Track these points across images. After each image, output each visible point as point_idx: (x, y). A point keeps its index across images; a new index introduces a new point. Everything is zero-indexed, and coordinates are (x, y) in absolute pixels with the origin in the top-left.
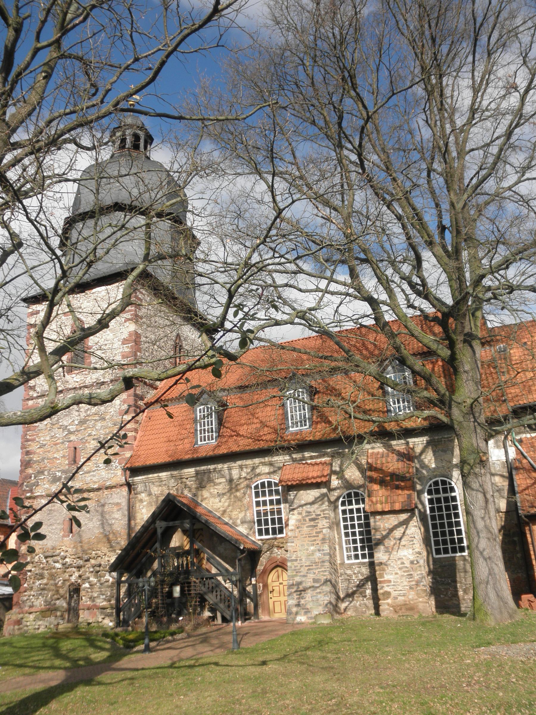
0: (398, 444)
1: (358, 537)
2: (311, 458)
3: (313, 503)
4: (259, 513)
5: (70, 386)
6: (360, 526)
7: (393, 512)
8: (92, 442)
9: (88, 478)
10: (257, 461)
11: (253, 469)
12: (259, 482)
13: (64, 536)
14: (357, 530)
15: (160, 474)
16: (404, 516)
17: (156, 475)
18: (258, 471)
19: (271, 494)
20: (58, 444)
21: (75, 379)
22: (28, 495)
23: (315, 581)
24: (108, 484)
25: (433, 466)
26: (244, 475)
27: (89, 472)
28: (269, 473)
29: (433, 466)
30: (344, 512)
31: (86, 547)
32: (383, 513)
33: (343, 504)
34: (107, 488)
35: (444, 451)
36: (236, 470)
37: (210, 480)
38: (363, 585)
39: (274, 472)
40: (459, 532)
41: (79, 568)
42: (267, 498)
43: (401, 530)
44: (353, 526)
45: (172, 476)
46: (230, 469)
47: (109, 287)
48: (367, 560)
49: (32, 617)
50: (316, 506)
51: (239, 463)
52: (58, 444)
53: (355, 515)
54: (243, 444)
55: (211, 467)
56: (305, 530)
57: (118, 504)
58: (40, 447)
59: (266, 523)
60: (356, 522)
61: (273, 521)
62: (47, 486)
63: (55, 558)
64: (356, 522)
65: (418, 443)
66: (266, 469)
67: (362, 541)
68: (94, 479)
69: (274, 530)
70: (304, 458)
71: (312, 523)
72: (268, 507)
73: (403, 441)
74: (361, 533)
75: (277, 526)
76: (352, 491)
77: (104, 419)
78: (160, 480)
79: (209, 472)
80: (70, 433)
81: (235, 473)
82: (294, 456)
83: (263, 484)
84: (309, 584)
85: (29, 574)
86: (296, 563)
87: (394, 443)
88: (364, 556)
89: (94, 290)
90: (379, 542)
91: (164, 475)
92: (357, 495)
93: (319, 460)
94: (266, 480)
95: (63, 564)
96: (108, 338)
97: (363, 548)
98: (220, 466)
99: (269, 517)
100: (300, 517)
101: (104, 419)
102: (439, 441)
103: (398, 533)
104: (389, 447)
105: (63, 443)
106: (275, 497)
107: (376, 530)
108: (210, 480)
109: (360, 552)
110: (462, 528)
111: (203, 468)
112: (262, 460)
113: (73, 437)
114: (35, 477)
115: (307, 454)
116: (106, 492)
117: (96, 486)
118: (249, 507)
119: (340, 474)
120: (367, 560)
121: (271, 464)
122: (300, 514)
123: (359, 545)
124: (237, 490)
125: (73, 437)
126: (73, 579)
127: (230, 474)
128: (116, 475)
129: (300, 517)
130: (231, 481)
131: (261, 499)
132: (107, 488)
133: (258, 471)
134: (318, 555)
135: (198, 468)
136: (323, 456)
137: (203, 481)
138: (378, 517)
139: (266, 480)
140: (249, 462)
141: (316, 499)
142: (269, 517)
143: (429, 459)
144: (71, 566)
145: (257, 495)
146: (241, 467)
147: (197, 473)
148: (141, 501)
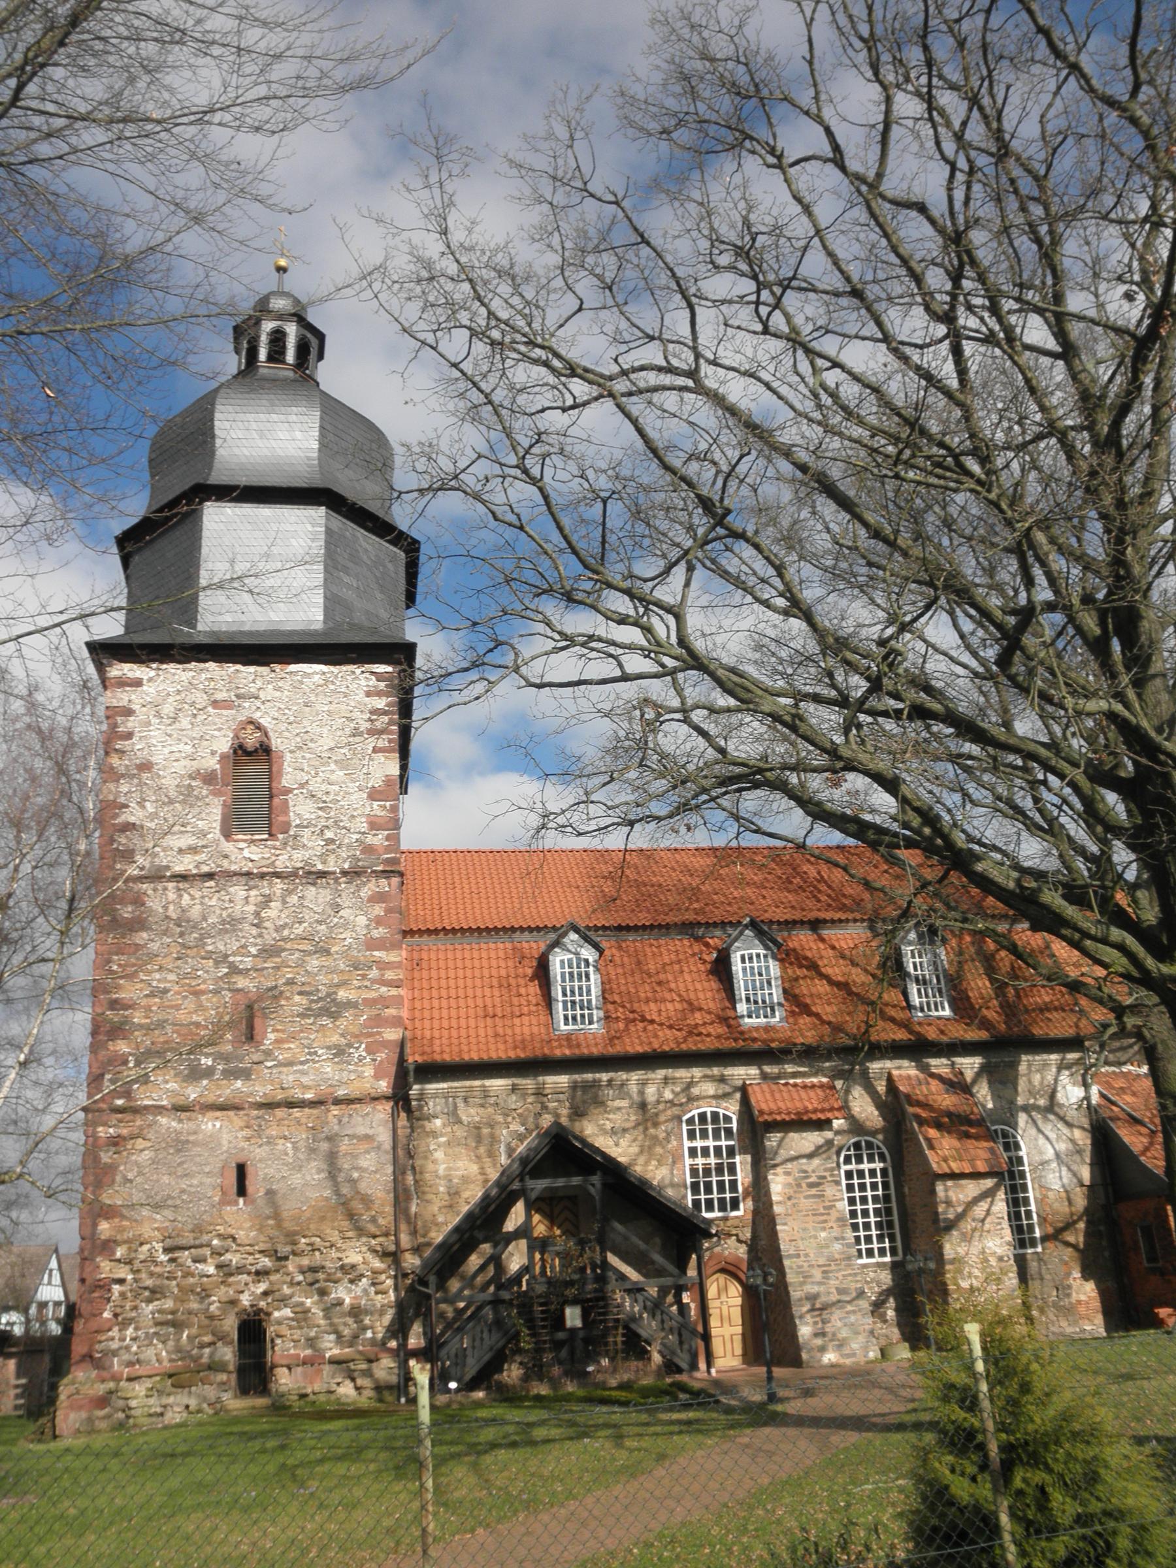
0: (939, 1065)
1: (872, 1219)
2: (795, 1075)
3: (810, 1156)
4: (694, 1171)
5: (233, 868)
6: (875, 1199)
7: (976, 1176)
8: (297, 998)
9: (288, 1077)
10: (697, 1072)
11: (690, 1085)
12: (695, 1112)
13: (223, 1202)
14: (871, 1206)
15: (488, 1082)
16: (989, 1183)
17: (477, 1083)
18: (695, 1091)
19: (717, 1137)
20: (203, 992)
21: (246, 853)
22: (120, 1102)
23: (840, 1291)
24: (341, 1092)
25: (990, 1105)
26: (668, 1095)
27: (290, 1064)
28: (715, 1097)
29: (990, 1105)
30: (849, 1175)
31: (289, 1225)
32: (953, 1176)
33: (848, 1160)
34: (337, 1102)
35: (1003, 1083)
36: (653, 1085)
37: (600, 1103)
38: (884, 1302)
39: (726, 1096)
40: (1029, 1214)
41: (261, 1274)
42: (710, 1143)
43: (984, 1205)
44: (864, 1200)
45: (514, 1089)
46: (643, 1083)
47: (335, 669)
48: (888, 1259)
49: (140, 1389)
50: (816, 1162)
51: (661, 1073)
52: (203, 992)
53: (868, 1180)
54: (666, 1040)
55: (604, 1077)
56: (805, 1204)
57: (368, 1138)
58: (152, 995)
59: (708, 1190)
60: (869, 1193)
61: (721, 1185)
62: (172, 1085)
63: (200, 1251)
64: (869, 1193)
65: (970, 1064)
66: (710, 1089)
67: (879, 1225)
68: (305, 1080)
69: (722, 1201)
70: (779, 1077)
71: (814, 1191)
72: (712, 1160)
73: (944, 1061)
74: (877, 1212)
75: (728, 1195)
76: (863, 1140)
77: (327, 952)
78: (485, 1093)
79: (596, 1084)
80: (235, 970)
81: (651, 1091)
82: (767, 1069)
83: (703, 1117)
84: (834, 1297)
85: (116, 1288)
86: (800, 1261)
87: (933, 1062)
88: (882, 1252)
89: (293, 667)
90: (950, 1226)
91: (497, 1084)
92: (870, 1145)
93: (808, 1081)
94: (709, 1110)
95: (219, 1267)
96: (333, 778)
97: (880, 1238)
98: (623, 1075)
99: (714, 1179)
100: (790, 1179)
101: (327, 952)
102: (997, 1066)
103: (980, 1210)
104: (925, 1069)
105: (216, 992)
106: (724, 1143)
107: (948, 1203)
108: (600, 1103)
109: (875, 1246)
110: (1033, 1207)
111: (589, 1076)
112: (708, 1071)
113: (241, 982)
114: (138, 1063)
115: (790, 1068)
116: (335, 1111)
117: (309, 1096)
118: (677, 1159)
119: (845, 1108)
120: (888, 1259)
121: (722, 1080)
122: (787, 1174)
123: (874, 1232)
124: (656, 1125)
125: (241, 982)
126: (245, 1300)
127: (641, 1093)
128: (360, 1077)
129: (790, 1179)
130: (643, 1106)
131: (699, 1143)
132: (337, 1102)
133: (695, 1091)
134: (837, 1246)
135: (577, 1077)
136: (815, 1074)
137: (586, 1101)
138: (950, 1183)
139: (709, 1110)
140: (682, 1073)
141: (818, 1148)
142: (714, 1179)
143: (983, 1093)
144: (240, 1270)
145: (692, 1135)
146: (666, 1080)
147: (574, 1087)
148: (434, 1134)
